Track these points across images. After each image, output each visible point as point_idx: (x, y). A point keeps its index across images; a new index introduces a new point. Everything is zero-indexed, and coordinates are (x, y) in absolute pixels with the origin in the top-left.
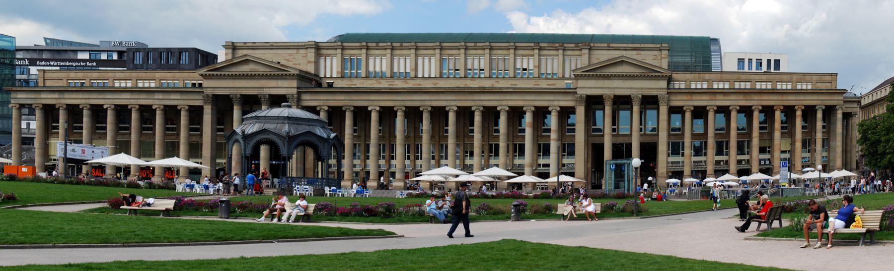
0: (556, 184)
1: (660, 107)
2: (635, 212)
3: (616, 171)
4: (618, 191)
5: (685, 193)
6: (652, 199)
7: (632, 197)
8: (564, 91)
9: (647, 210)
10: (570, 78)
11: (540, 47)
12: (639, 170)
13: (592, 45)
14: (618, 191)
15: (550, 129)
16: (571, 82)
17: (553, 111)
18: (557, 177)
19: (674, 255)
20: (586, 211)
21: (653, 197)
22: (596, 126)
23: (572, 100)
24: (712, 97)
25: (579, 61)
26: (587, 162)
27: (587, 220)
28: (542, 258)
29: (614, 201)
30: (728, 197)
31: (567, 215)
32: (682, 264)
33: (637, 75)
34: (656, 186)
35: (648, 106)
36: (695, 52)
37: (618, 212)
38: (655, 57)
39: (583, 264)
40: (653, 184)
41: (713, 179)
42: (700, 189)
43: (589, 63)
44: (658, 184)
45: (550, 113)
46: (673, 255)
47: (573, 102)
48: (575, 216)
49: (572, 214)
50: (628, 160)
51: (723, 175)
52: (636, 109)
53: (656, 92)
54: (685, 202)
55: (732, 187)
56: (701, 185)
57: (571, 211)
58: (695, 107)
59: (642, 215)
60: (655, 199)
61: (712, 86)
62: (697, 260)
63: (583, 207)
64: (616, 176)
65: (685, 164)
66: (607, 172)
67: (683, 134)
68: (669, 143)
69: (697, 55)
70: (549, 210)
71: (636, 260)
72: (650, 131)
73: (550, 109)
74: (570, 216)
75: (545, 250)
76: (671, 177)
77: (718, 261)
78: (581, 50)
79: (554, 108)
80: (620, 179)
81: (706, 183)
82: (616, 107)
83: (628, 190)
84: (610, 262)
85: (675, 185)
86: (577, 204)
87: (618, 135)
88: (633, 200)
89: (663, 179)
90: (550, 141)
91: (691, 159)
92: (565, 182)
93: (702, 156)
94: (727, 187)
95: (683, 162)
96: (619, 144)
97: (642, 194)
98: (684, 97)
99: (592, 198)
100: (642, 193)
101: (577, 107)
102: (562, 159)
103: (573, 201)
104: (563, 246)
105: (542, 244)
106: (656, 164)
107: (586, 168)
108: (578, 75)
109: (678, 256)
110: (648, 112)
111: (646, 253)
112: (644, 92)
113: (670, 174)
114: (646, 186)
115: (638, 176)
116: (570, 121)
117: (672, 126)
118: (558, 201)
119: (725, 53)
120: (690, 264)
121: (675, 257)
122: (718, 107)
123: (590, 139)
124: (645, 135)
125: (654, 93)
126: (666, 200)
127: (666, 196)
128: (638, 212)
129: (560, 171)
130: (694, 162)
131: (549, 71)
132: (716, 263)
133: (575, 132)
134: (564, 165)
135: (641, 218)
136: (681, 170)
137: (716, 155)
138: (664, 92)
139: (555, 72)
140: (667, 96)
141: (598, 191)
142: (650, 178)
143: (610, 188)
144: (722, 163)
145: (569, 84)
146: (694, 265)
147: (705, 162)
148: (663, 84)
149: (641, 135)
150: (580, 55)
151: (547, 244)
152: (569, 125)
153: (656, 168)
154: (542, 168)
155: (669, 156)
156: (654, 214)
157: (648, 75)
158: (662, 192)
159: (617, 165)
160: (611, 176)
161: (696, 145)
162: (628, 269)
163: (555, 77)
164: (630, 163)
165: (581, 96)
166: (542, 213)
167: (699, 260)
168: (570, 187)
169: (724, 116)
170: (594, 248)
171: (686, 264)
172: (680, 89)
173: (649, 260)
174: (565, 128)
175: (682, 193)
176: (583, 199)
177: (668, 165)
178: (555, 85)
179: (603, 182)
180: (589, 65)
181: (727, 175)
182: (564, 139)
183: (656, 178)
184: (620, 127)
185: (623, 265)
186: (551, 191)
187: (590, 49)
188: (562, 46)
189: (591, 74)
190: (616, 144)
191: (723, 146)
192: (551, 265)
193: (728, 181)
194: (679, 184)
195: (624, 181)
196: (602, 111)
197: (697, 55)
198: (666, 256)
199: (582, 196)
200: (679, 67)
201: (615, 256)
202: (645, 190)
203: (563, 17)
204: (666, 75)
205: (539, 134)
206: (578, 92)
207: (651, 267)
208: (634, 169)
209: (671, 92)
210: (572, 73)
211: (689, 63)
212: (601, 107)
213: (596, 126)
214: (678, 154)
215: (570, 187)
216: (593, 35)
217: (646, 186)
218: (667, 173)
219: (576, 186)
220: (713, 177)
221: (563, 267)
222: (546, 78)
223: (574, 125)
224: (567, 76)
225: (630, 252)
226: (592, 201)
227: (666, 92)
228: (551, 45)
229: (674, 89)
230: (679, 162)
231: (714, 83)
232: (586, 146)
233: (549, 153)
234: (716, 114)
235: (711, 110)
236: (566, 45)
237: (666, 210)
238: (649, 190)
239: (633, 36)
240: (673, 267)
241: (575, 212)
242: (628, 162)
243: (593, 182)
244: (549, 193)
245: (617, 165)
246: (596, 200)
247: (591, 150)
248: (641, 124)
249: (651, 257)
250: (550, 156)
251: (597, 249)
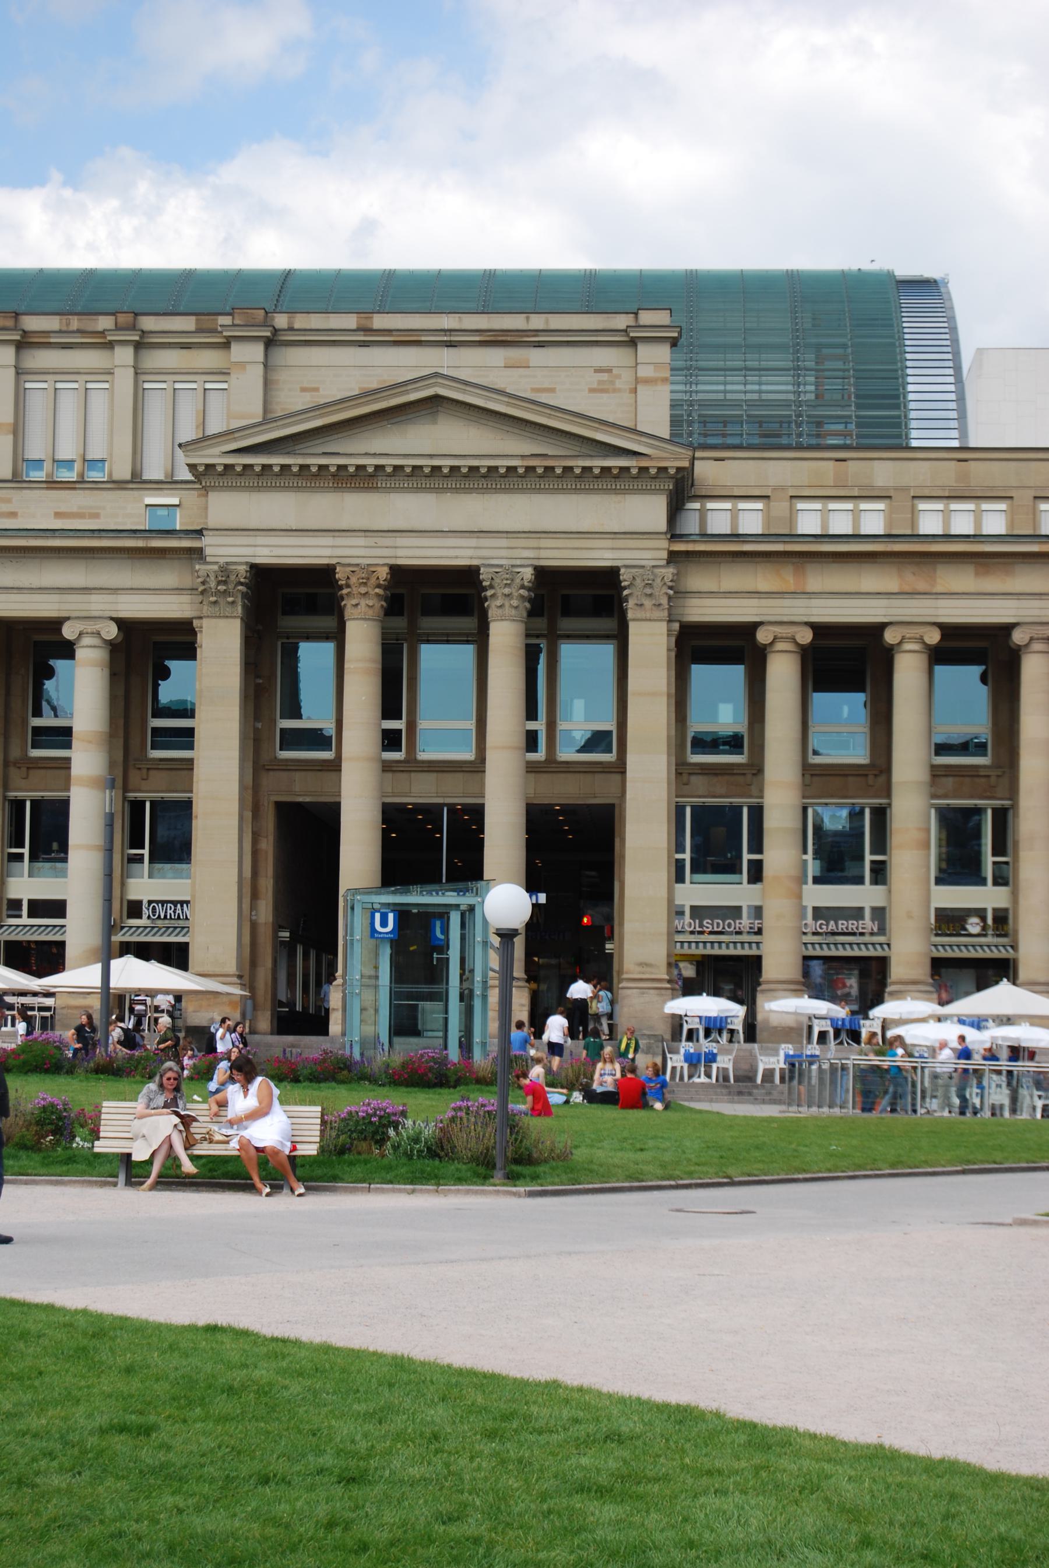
0: (95, 1003)
1: (633, 628)
2: (499, 1163)
3: (399, 944)
4: (408, 1048)
5: (769, 1075)
6: (591, 1097)
7: (483, 1081)
8: (140, 543)
9: (564, 1157)
10: (170, 483)
11: (25, 333)
12: (519, 943)
13: (281, 321)
14: (408, 1048)
15: (67, 731)
16: (176, 501)
17: (86, 641)
18: (98, 968)
19: (713, 1406)
20: (244, 1145)
21: (596, 1087)
22: (299, 716)
23: (178, 590)
24: (912, 579)
25: (215, 402)
26: (255, 895)
27: (249, 1188)
28: (14, 1377)
29: (391, 1099)
30: (1014, 1111)
31: (150, 1162)
32: (758, 1459)
33: (511, 469)
34: (611, 1027)
35: (567, 624)
36: (819, 347)
37: (410, 1157)
38: (605, 376)
39: (224, 1419)
40: (597, 1017)
41: (927, 1007)
42: (856, 1057)
43: (266, 410)
44: (623, 1021)
45: (67, 650)
46: (706, 1400)
47: (186, 598)
48: (188, 1167)
49: (171, 1156)
50: (465, 891)
51: (982, 985)
53: (608, 554)
54: (770, 1120)
55: (1032, 1055)
56: (855, 1036)
57: (169, 1140)
58: (819, 629)
59: (535, 1178)
60: (608, 1098)
61: (914, 522)
62: (845, 1444)
63: (231, 1123)
64: (399, 974)
65: (769, 921)
66: (357, 948)
67: (756, 768)
68: (680, 810)
69: (829, 365)
70: (57, 1131)
71: (507, 1417)
72: (583, 749)
73: (68, 632)
74: (163, 1165)
75: (24, 1336)
76: (690, 988)
77: (962, 1458)
78: (226, 345)
79: (90, 627)
80: (425, 988)
81: (885, 1025)
82: (400, 623)
83: (466, 1045)
84: (368, 1416)
85: (713, 1027)
86: (197, 1107)
87: (413, 766)
88: (487, 1099)
89: (652, 996)
90: (68, 789)
91: (800, 897)
92: (138, 992)
93: (859, 880)
94: (1004, 1054)
95: (758, 912)
96: (419, 808)
97: (537, 1072)
98: (762, 579)
99: (278, 1078)
100: (538, 1061)
101: (205, 622)
102: (125, 875)
103: (177, 1089)
104: (124, 1319)
105: (13, 1303)
106: (610, 918)
107: (249, 927)
108: (209, 467)
109: (736, 1410)
110: (568, 651)
111: (555, 1385)
112: (543, 554)
113: (689, 971)
114: (556, 1027)
115: (519, 971)
116: (168, 692)
117: (697, 725)
118: (105, 1085)
119: (980, 351)
120: (806, 1463)
121: (718, 1415)
122: (949, 631)
123: (269, 780)
124: (551, 766)
126: (667, 1107)
127: (664, 1085)
128: (518, 1161)
129: (118, 938)
130: (819, 913)
131: (67, 450)
132: (951, 1468)
133: (190, 746)
134: (134, 909)
135: (531, 1194)
136: (747, 952)
137: (939, 881)
138: (654, 553)
139: (94, 454)
140: (669, 572)
141: (310, 1046)
142: (580, 990)
143: (369, 1030)
144: (973, 926)
145: (163, 512)
146: (827, 1466)
147: (879, 913)
149: (532, 768)
150: (223, 373)
151: (38, 1306)
152: (160, 712)
153: (611, 938)
154: (25, 920)
155: (680, 878)
156: (605, 1177)
157: (568, 469)
158: (644, 1062)
159: (404, 914)
160: (376, 968)
161: (829, 825)
162: (463, 1462)
163: (94, 475)
164: (472, 909)
165: (225, 572)
166: (24, 1147)
167: (857, 1447)
168: (165, 1020)
169: (984, 679)
170: (284, 1341)
171: (784, 1462)
172: (735, 537)
173: (576, 1421)
174: (144, 722)
175: (756, 1072)
176: (232, 1080)
177: (678, 924)
178: (96, 516)
179: (334, 998)
180: (268, 419)
181: (1004, 987)
182: (134, 777)
183: (610, 989)
184: (423, 724)
185: (436, 1437)
186: (69, 1034)
187: (270, 343)
188: (133, 327)
189: (276, 460)
190: (400, 808)
191: (978, 834)
192: (65, 1419)
193: (1007, 1020)
194: (738, 1025)
195: (442, 997)
196: (330, 647)
197: (829, 365)
198: (664, 1409)
199: (224, 1065)
200: (730, 429)
201: (391, 1385)
202: (555, 1049)
203: (143, 188)
204: (663, 470)
205: (15, 753)
206: (208, 551)
207: (584, 1461)
208: (496, 941)
210: (182, 459)
211: (786, 404)
212: (327, 622)
213: (299, 716)
214: (731, 867)
215: (165, 1020)
216: (288, 274)
217: (556, 1027)
218: (672, 964)
219: (196, 1015)
220: (925, 996)
221: (123, 1429)
222: (52, 484)
223: (187, 711)
224: (154, 471)
225: (472, 1373)
226: (276, 1092)
227: (664, 555)
228: (75, 323)
229: (705, 536)
230: (735, 912)
231: (922, 506)
232: (249, 815)
233: (64, 848)
234: (938, 669)
235: (908, 646)
236: (148, 323)
237: (667, 1157)
238: (577, 1048)
239: (490, 276)
240: (709, 1473)
241: (188, 1145)
242: (465, 901)
243: (283, 996)
244: (61, 1046)
245: (404, 914)
246: (297, 1091)
247: (271, 838)
248: (531, 713)
249: (587, 1407)
250: (65, 860)
251: (297, 1343)
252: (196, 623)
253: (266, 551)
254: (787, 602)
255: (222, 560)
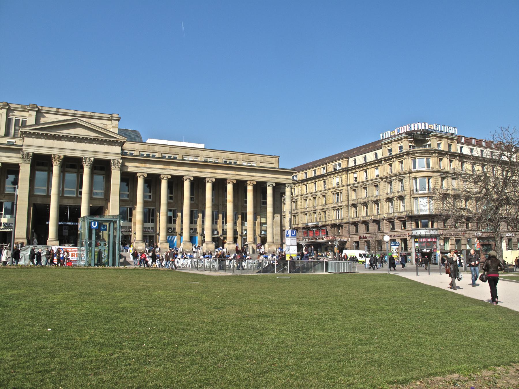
52: (56, 169)
108: (26, 132)
112: (96, 156)
125: (107, 157)
138: (118, 158)
148: (117, 149)
157: (102, 140)
206: (24, 149)
209: (126, 158)
227: (120, 158)
252: (20, 164)
253: (37, 150)
254: (143, 169)
255: (27, 152)
